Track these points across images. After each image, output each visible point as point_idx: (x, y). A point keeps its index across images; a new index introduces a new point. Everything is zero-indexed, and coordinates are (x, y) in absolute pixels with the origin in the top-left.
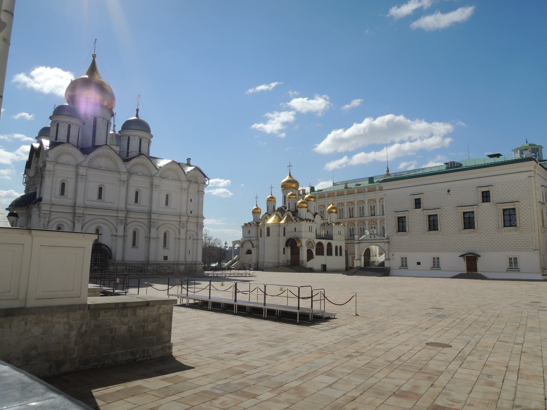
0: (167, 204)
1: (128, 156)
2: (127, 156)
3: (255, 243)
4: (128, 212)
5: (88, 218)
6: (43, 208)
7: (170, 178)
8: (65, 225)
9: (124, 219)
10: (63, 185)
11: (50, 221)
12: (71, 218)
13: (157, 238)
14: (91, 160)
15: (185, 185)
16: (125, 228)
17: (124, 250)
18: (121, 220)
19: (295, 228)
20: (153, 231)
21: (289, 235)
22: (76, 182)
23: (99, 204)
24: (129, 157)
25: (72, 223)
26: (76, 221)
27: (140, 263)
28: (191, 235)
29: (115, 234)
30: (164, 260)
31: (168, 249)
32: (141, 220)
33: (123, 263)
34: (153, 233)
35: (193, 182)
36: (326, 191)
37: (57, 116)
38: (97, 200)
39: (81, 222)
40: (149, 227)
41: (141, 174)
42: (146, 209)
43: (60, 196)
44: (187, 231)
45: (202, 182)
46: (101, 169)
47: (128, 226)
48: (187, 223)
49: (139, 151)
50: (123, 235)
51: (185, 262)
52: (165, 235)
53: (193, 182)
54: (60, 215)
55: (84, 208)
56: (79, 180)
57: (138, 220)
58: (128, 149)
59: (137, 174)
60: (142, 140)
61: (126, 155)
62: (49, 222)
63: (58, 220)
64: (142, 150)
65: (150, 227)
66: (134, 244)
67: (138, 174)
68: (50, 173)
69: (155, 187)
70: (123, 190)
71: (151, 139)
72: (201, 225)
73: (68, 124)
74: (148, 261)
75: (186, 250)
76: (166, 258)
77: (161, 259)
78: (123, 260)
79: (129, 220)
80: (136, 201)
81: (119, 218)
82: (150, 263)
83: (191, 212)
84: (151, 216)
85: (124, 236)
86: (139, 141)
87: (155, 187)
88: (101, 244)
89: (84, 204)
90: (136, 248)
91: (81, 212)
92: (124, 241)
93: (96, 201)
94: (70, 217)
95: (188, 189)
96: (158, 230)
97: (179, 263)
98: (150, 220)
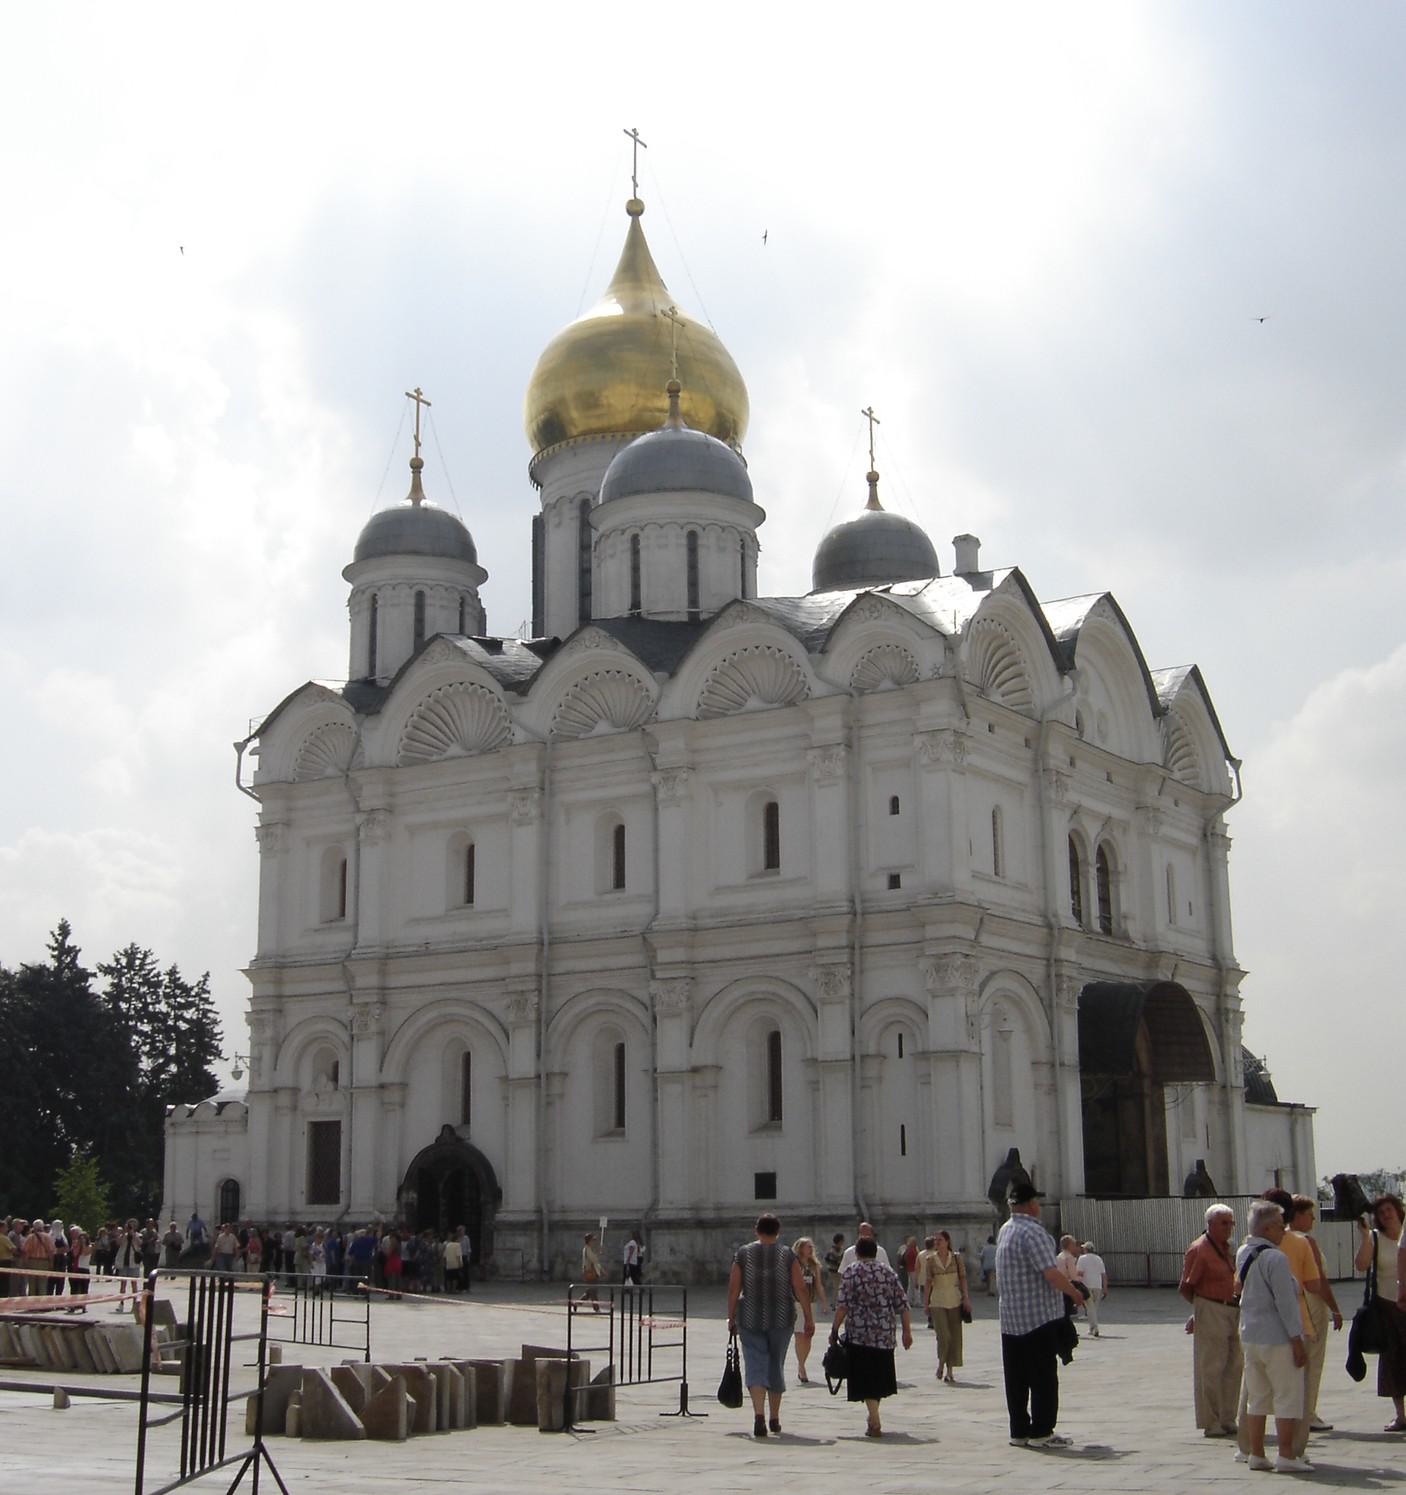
9: (533, 986)
13: (695, 1070)
22: (358, 850)
28: (896, 1030)
30: (758, 1196)
33: (547, 1224)
42: (642, 911)
43: (325, 925)
47: (564, 1020)
50: (533, 1075)
51: (857, 1205)
70: (527, 838)
75: (857, 1132)
76: (765, 1185)
77: (739, 1193)
78: (539, 1211)
82: (663, 1215)
83: (894, 882)
85: (538, 1077)
86: (627, 557)
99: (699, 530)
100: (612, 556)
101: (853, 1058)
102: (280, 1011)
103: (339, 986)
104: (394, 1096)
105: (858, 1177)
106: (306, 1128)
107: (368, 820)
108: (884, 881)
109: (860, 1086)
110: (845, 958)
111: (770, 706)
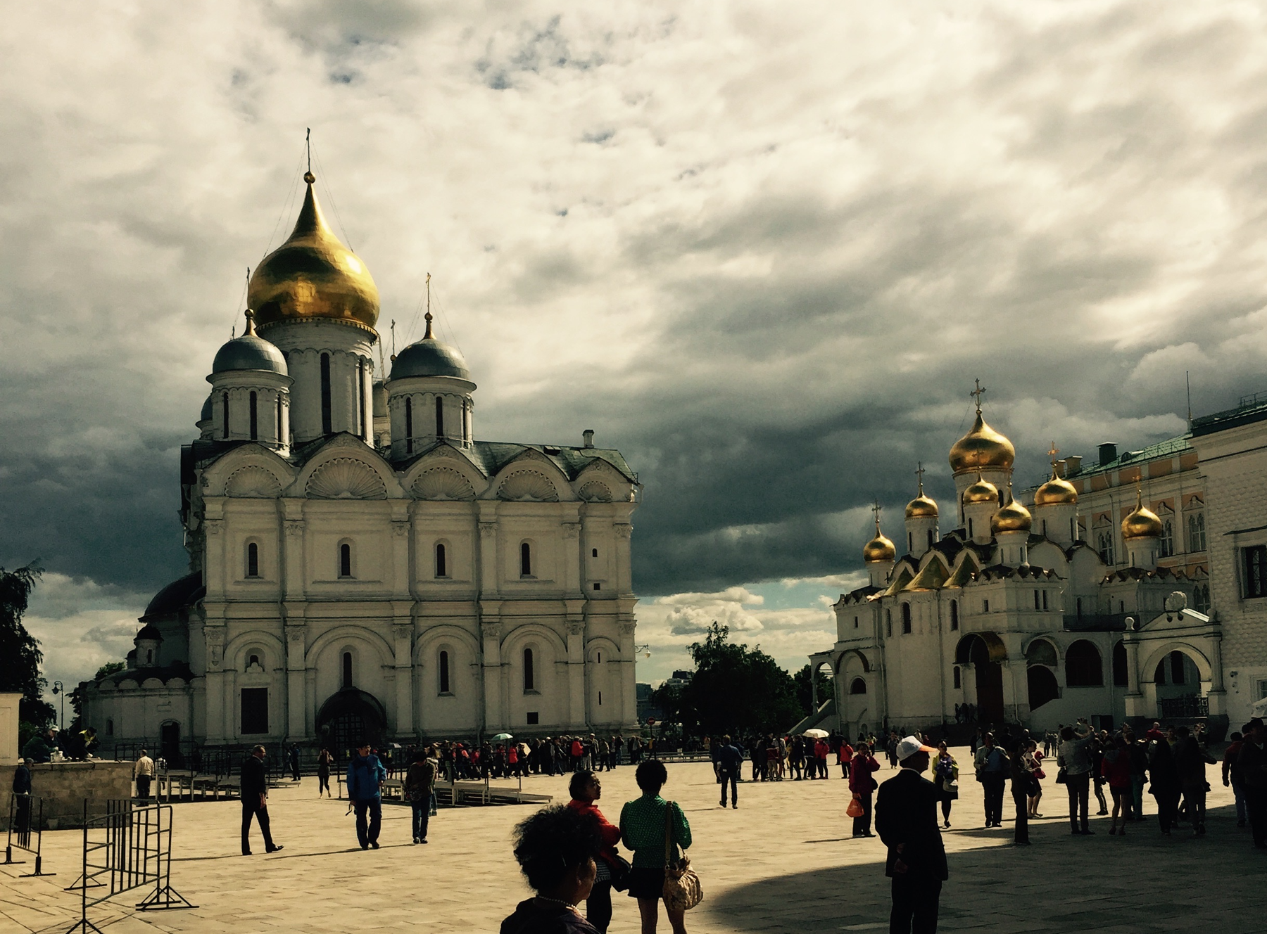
0: (526, 569)
1: (410, 451)
2: (408, 453)
3: (870, 656)
4: (417, 601)
5: (317, 628)
6: (209, 614)
7: (528, 497)
8: (266, 650)
10: (252, 550)
11: (230, 643)
12: (278, 632)
13: (502, 665)
14: (313, 477)
15: (572, 511)
16: (413, 645)
17: (416, 702)
18: (401, 624)
19: (986, 602)
20: (491, 649)
21: (970, 626)
22: (281, 540)
23: (343, 588)
24: (414, 455)
25: (282, 643)
26: (289, 639)
27: (449, 734)
29: (389, 662)
30: (528, 723)
31: (537, 693)
32: (454, 621)
34: (492, 653)
35: (595, 499)
36: (1161, 453)
37: (222, 374)
38: (339, 578)
39: (302, 638)
40: (479, 638)
41: (444, 497)
44: (587, 640)
45: (621, 499)
46: (340, 496)
47: (423, 640)
48: (584, 618)
49: (438, 435)
51: (587, 726)
52: (528, 655)
53: (595, 499)
54: (252, 625)
55: (306, 604)
56: (288, 532)
57: (446, 622)
58: (409, 433)
59: (435, 498)
60: (444, 402)
61: (405, 450)
62: (225, 647)
63: (248, 638)
64: (444, 429)
65: (482, 638)
66: (444, 685)
67: (438, 498)
68: (217, 525)
69: (486, 528)
70: (401, 547)
71: (472, 395)
72: (627, 621)
73: (250, 390)
74: (484, 729)
75: (587, 694)
76: (533, 718)
79: (423, 624)
80: (441, 570)
81: (396, 622)
83: (597, 587)
84: (480, 608)
87: (486, 528)
88: (357, 693)
89: (304, 592)
90: (451, 695)
91: (300, 613)
92: (415, 682)
93: (338, 582)
94: (275, 628)
95: (581, 522)
96: (505, 645)
97: (570, 729)
98: (480, 619)
99: (443, 396)
100: (424, 404)
101: (585, 662)
102: (225, 625)
103: (276, 614)
104: (311, 675)
105: (588, 714)
106: (240, 692)
107: (292, 526)
108: (591, 586)
109: (586, 674)
110: (580, 618)
111: (534, 499)
